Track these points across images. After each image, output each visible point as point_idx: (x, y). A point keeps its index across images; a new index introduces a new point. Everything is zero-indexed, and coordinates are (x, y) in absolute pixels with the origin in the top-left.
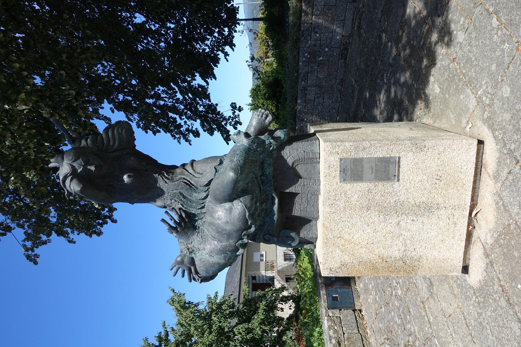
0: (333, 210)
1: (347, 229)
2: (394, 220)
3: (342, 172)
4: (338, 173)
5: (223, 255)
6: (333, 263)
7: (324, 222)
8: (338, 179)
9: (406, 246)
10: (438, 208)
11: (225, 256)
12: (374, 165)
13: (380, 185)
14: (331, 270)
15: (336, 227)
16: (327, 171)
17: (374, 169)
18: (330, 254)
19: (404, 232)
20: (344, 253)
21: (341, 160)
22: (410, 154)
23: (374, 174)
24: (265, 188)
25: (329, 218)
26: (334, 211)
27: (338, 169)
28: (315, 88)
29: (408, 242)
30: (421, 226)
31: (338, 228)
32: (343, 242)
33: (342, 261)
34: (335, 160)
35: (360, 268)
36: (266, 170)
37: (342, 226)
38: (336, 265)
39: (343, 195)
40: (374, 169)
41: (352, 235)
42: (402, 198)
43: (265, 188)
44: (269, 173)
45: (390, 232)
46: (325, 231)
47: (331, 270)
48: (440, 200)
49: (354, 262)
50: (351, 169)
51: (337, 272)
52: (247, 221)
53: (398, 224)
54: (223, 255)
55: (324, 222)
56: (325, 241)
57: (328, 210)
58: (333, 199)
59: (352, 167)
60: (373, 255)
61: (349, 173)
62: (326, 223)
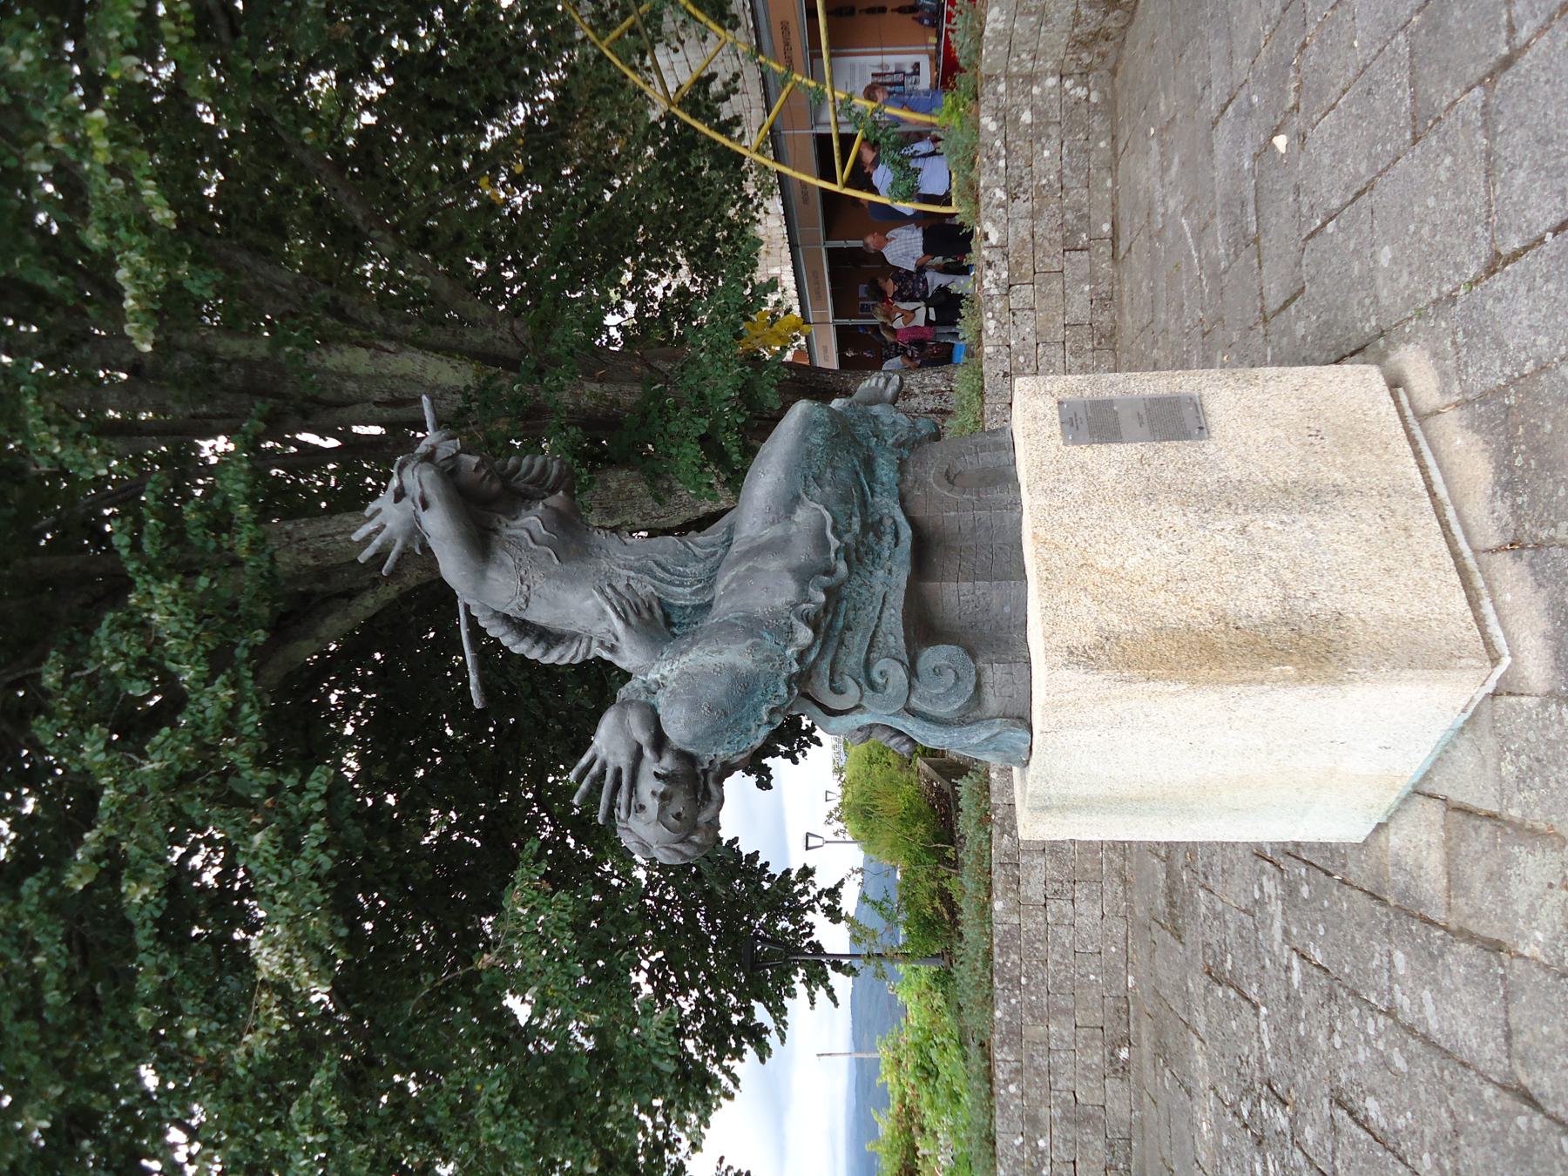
0: (1057, 503)
1: (1102, 546)
2: (1229, 522)
3: (1067, 427)
4: (1057, 429)
5: (749, 642)
6: (1076, 633)
8: (1058, 440)
9: (1284, 585)
10: (1339, 493)
11: (754, 645)
12: (1142, 411)
13: (1170, 449)
14: (1071, 653)
16: (1029, 425)
19: (1265, 551)
21: (1060, 403)
22: (1225, 392)
23: (1146, 428)
27: (1057, 421)
28: (1041, 860)
29: (1288, 576)
30: (1309, 536)
32: (1096, 577)
33: (1100, 629)
34: (1046, 407)
35: (1161, 645)
38: (1084, 640)
39: (1077, 470)
41: (1119, 560)
42: (1235, 475)
45: (1226, 551)
47: (1071, 653)
48: (1339, 477)
49: (1139, 629)
52: (826, 545)
53: (1243, 531)
54: (749, 642)
56: (1045, 574)
57: (1043, 501)
60: (1194, 612)
61: (1084, 427)
62: (1041, 532)
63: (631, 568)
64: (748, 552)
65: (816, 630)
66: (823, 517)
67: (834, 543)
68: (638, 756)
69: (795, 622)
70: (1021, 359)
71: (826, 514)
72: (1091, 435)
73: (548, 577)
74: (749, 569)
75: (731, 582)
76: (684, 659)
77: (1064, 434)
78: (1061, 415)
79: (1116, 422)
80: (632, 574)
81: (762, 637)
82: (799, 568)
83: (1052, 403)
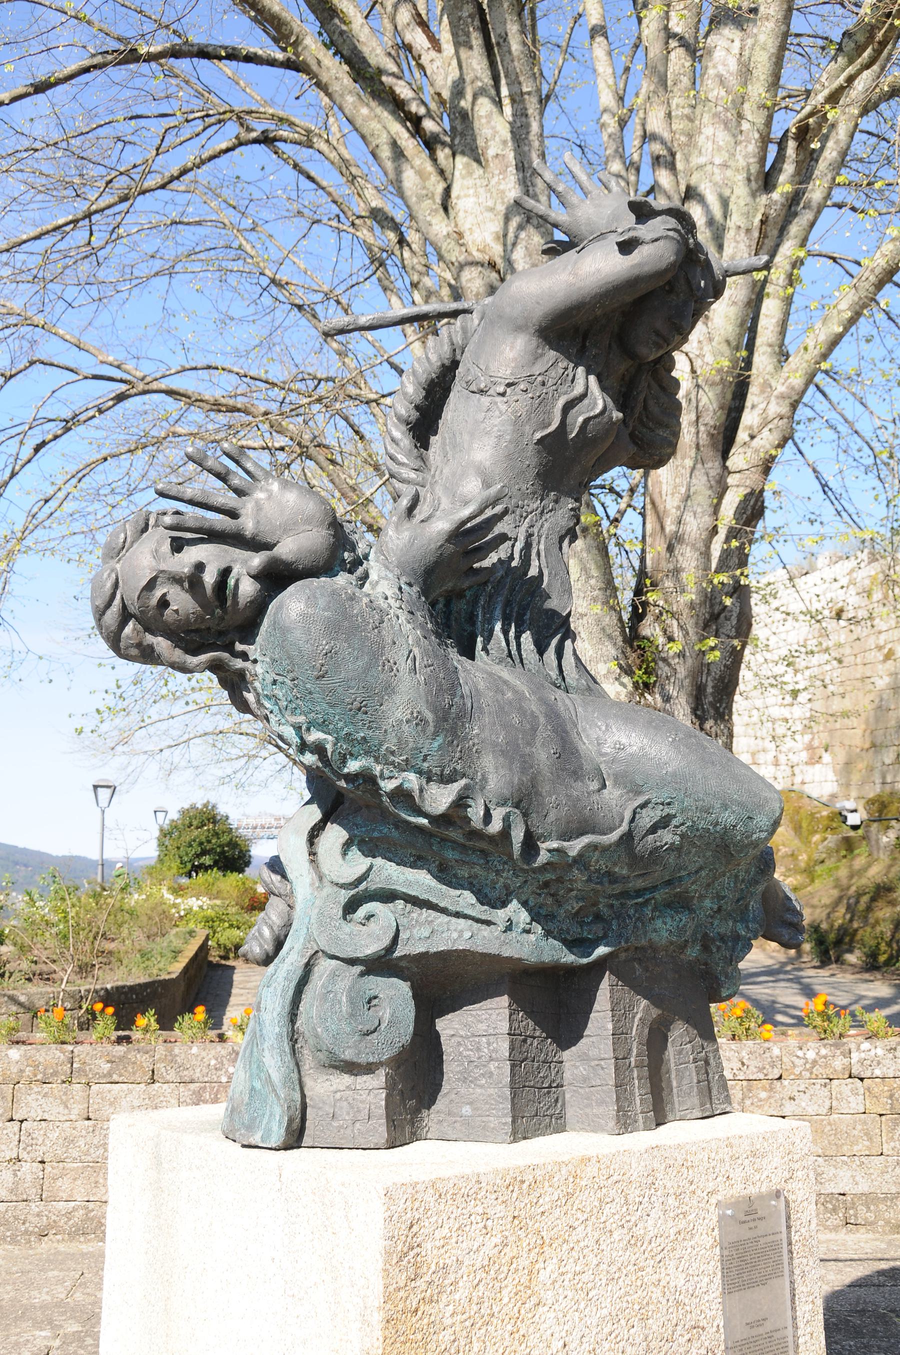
0: (634, 1194)
4: (738, 1190)
7: (594, 1160)
11: (422, 722)
15: (579, 1215)
17: (761, 1330)
18: (480, 1210)
20: (480, 1274)
24: (631, 912)
25: (610, 1181)
26: (631, 1198)
27: (753, 1190)
31: (576, 1224)
36: (668, 920)
37: (582, 1244)
40: (761, 1330)
41: (549, 1296)
43: (631, 912)
44: (655, 930)
46: (564, 1171)
50: (756, 1240)
51: (400, 1259)
54: (429, 716)
55: (594, 1160)
56: (529, 1178)
58: (669, 1185)
59: (762, 1241)
62: (591, 1170)
63: (528, 546)
64: (558, 716)
65: (443, 820)
66: (612, 830)
67: (575, 847)
68: (254, 544)
69: (457, 786)
70: (763, 1095)
71: (614, 836)
72: (734, 1245)
73: (517, 422)
74: (534, 717)
75: (516, 692)
76: (403, 617)
77: (735, 1204)
78: (761, 1197)
79: (752, 1284)
80: (519, 546)
81: (436, 734)
82: (538, 794)
83: (776, 1183)
